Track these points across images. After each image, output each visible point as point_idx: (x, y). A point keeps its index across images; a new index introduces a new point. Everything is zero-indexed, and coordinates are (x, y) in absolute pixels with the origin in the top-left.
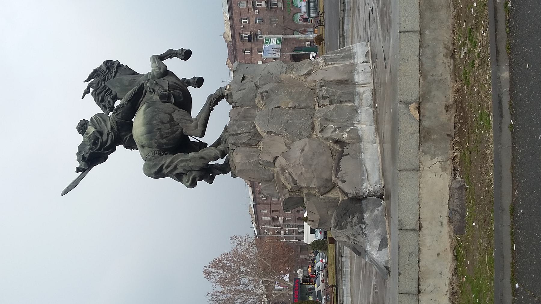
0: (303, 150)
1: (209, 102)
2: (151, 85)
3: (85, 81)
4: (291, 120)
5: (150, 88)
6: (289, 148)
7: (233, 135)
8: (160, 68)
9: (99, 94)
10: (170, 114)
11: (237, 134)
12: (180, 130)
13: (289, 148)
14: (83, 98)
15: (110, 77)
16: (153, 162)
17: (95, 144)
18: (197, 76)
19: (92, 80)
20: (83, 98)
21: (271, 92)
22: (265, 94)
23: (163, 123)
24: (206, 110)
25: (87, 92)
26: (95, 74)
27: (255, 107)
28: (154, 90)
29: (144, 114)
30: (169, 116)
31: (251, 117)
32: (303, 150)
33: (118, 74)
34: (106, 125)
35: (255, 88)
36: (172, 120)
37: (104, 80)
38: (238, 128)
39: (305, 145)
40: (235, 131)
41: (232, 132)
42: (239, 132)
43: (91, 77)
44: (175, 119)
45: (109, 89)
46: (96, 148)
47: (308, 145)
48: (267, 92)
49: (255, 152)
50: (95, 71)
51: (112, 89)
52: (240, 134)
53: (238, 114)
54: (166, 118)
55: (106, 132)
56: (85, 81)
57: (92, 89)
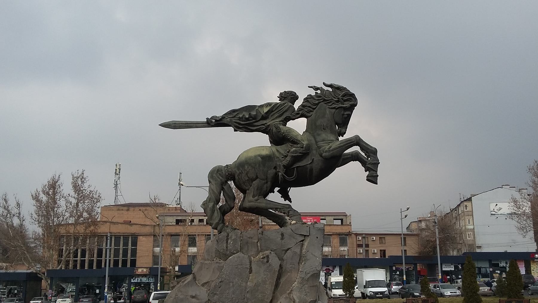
0: (193, 297)
2: (291, 152)
3: (324, 84)
4: (233, 286)
5: (288, 152)
6: (203, 285)
7: (228, 236)
9: (308, 101)
10: (257, 177)
11: (227, 240)
12: (247, 188)
13: (203, 285)
15: (330, 104)
16: (216, 174)
17: (247, 119)
18: (379, 179)
19: (330, 89)
21: (268, 264)
22: (265, 260)
23: (247, 174)
24: (272, 206)
25: (316, 89)
26: (337, 88)
27: (258, 252)
28: (286, 156)
29: (255, 156)
31: (248, 249)
32: (193, 297)
33: (334, 110)
34: (273, 120)
35: (286, 248)
36: (253, 180)
37: (325, 100)
39: (198, 299)
40: (231, 237)
42: (229, 241)
43: (330, 86)
44: (254, 182)
45: (314, 109)
47: (198, 301)
48: (268, 262)
49: (212, 256)
50: (339, 88)
51: (315, 111)
52: (227, 242)
53: (249, 238)
54: (252, 175)
55: (265, 122)
56: (324, 84)
57: (319, 92)
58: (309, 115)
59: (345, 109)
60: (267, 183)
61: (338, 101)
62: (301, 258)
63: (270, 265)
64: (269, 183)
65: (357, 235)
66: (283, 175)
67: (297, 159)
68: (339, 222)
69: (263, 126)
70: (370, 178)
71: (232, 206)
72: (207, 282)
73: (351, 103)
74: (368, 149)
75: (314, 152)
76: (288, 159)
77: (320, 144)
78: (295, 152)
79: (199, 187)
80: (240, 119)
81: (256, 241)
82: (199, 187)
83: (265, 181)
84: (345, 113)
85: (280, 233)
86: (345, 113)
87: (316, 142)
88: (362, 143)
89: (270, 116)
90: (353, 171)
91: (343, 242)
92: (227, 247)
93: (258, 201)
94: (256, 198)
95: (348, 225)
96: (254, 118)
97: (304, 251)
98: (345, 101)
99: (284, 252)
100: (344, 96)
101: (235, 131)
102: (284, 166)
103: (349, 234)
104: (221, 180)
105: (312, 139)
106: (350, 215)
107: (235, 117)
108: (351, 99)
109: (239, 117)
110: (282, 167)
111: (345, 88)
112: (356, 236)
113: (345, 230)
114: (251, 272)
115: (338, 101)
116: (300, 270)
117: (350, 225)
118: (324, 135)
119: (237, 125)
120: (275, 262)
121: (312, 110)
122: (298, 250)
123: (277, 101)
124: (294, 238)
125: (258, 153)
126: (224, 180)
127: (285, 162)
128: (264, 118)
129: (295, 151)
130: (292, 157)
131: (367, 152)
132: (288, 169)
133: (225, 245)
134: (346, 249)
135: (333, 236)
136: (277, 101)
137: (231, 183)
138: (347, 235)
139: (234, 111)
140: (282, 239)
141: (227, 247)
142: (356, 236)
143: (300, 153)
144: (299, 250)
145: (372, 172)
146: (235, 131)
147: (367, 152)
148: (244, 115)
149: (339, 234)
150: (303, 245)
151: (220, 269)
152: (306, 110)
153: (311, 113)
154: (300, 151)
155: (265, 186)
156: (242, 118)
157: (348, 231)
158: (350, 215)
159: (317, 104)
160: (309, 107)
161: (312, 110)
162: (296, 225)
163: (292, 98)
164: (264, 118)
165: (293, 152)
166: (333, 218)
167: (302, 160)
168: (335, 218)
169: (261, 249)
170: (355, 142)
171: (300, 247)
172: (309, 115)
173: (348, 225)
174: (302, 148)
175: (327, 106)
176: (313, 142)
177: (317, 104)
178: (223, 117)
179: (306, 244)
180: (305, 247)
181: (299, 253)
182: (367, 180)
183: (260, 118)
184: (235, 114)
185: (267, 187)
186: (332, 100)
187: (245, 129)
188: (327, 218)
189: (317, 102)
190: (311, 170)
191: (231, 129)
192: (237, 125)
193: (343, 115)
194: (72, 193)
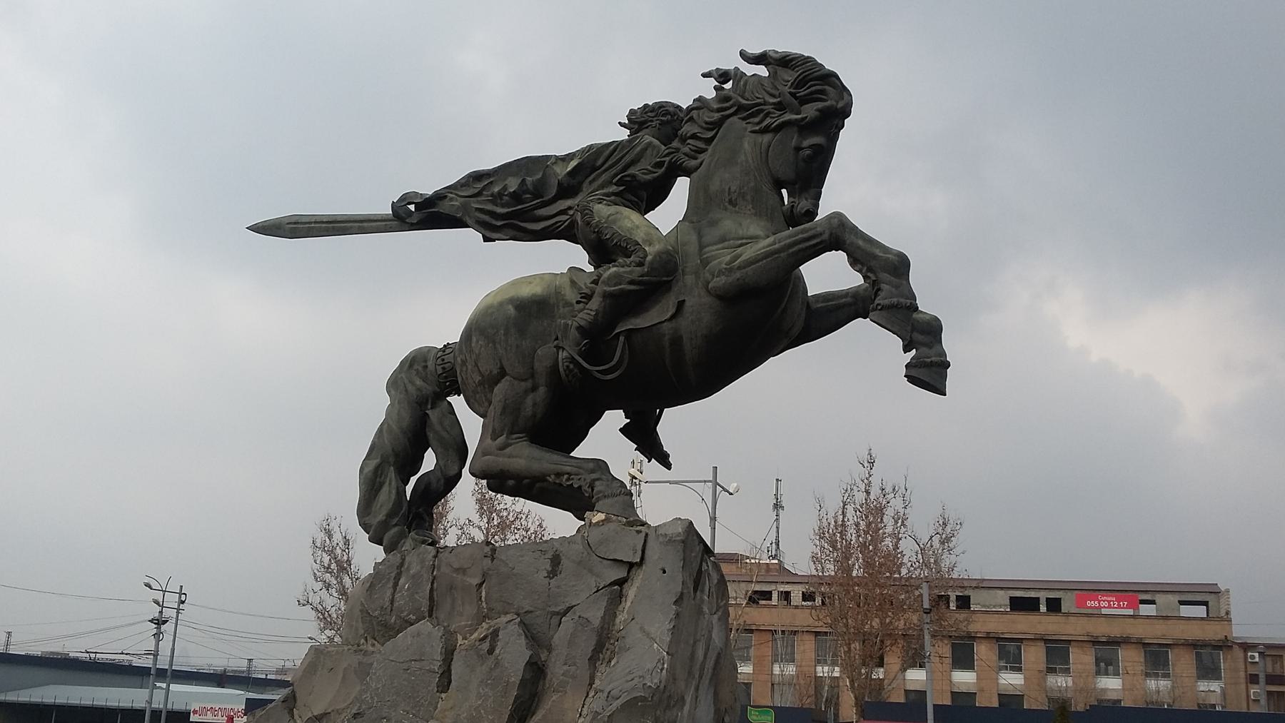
1: (568, 469)
3: (743, 55)
7: (402, 564)
8: (721, 273)
10: (503, 373)
14: (704, 75)
15: (757, 120)
17: (516, 197)
20: (704, 75)
21: (492, 658)
22: (486, 646)
25: (723, 76)
28: (588, 297)
29: (501, 304)
30: (495, 372)
33: (767, 138)
37: (741, 108)
38: (413, 576)
41: (407, 559)
42: (402, 581)
46: (503, 206)
48: (491, 651)
51: (710, 149)
52: (396, 584)
53: (457, 570)
55: (569, 203)
56: (743, 55)
58: (693, 163)
59: (806, 128)
60: (534, 389)
61: (780, 107)
62: (604, 644)
63: (497, 664)
64: (542, 390)
65: (1246, 647)
66: (573, 360)
67: (626, 302)
68: (1200, 611)
69: (564, 217)
70: (914, 373)
71: (453, 472)
72: (326, 714)
73: (820, 105)
74: (875, 257)
75: (689, 279)
76: (595, 304)
77: (711, 250)
78: (617, 278)
79: (676, 483)
80: (496, 198)
81: (476, 581)
82: (676, 483)
83: (529, 384)
84: (806, 143)
85: (549, 555)
86: (806, 143)
87: (701, 247)
88: (849, 238)
89: (585, 185)
90: (869, 347)
91: (1208, 671)
92: (392, 602)
93: (508, 450)
94: (501, 440)
95: (1221, 619)
96: (538, 191)
97: (621, 618)
98: (804, 101)
99: (555, 620)
100: (799, 84)
101: (486, 239)
102: (580, 328)
103: (1225, 645)
104: (419, 389)
105: (694, 238)
106: (1227, 591)
107: (479, 194)
108: (822, 92)
109: (492, 195)
110: (573, 333)
111: (808, 60)
112: (1245, 651)
113: (1212, 632)
114: (445, 682)
115: (780, 107)
116: (597, 682)
117: (1226, 619)
118: (728, 224)
119: (487, 218)
120: (515, 653)
121: (701, 145)
122: (596, 615)
123: (624, 134)
124: (591, 571)
125: (512, 293)
126: (429, 389)
127: (585, 316)
128: (568, 189)
129: (616, 275)
130: (606, 296)
131: (870, 269)
132: (596, 338)
133: (389, 593)
134: (1215, 686)
135: (1176, 651)
136: (624, 134)
137: (458, 402)
138: (1219, 648)
139: (477, 176)
140: (553, 573)
141: (392, 602)
142: (1245, 651)
143: (631, 282)
144: (601, 613)
145: (924, 350)
146: (486, 239)
147: (870, 269)
148: (505, 188)
149: (1194, 645)
150: (620, 596)
151: (363, 671)
152: (686, 149)
153: (702, 157)
154: (634, 277)
155: (529, 400)
156: (500, 194)
157: (1220, 636)
158: (1227, 591)
159: (717, 125)
160: (694, 136)
161: (701, 145)
162: (605, 529)
163: (662, 123)
164: (568, 189)
165: (607, 283)
166: (1176, 598)
167: (646, 310)
168: (1184, 598)
169: (490, 609)
170: (826, 236)
171: (603, 603)
172: (693, 163)
173: (1221, 619)
174: (641, 264)
175: (750, 128)
176: (693, 248)
177: (717, 125)
178: (439, 196)
179: (631, 592)
180: (629, 604)
181: (596, 622)
182: (912, 379)
183: (553, 191)
184: (480, 186)
185: (535, 404)
186: (765, 103)
187: (512, 233)
188: (1159, 598)
189: (717, 116)
190: (677, 341)
191: (471, 235)
192: (487, 218)
193: (798, 149)
194: (475, 518)
